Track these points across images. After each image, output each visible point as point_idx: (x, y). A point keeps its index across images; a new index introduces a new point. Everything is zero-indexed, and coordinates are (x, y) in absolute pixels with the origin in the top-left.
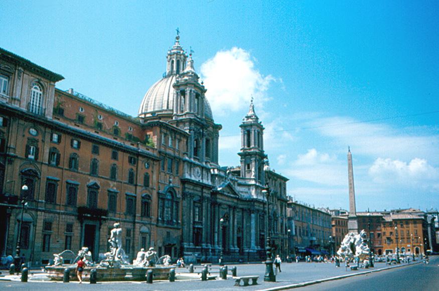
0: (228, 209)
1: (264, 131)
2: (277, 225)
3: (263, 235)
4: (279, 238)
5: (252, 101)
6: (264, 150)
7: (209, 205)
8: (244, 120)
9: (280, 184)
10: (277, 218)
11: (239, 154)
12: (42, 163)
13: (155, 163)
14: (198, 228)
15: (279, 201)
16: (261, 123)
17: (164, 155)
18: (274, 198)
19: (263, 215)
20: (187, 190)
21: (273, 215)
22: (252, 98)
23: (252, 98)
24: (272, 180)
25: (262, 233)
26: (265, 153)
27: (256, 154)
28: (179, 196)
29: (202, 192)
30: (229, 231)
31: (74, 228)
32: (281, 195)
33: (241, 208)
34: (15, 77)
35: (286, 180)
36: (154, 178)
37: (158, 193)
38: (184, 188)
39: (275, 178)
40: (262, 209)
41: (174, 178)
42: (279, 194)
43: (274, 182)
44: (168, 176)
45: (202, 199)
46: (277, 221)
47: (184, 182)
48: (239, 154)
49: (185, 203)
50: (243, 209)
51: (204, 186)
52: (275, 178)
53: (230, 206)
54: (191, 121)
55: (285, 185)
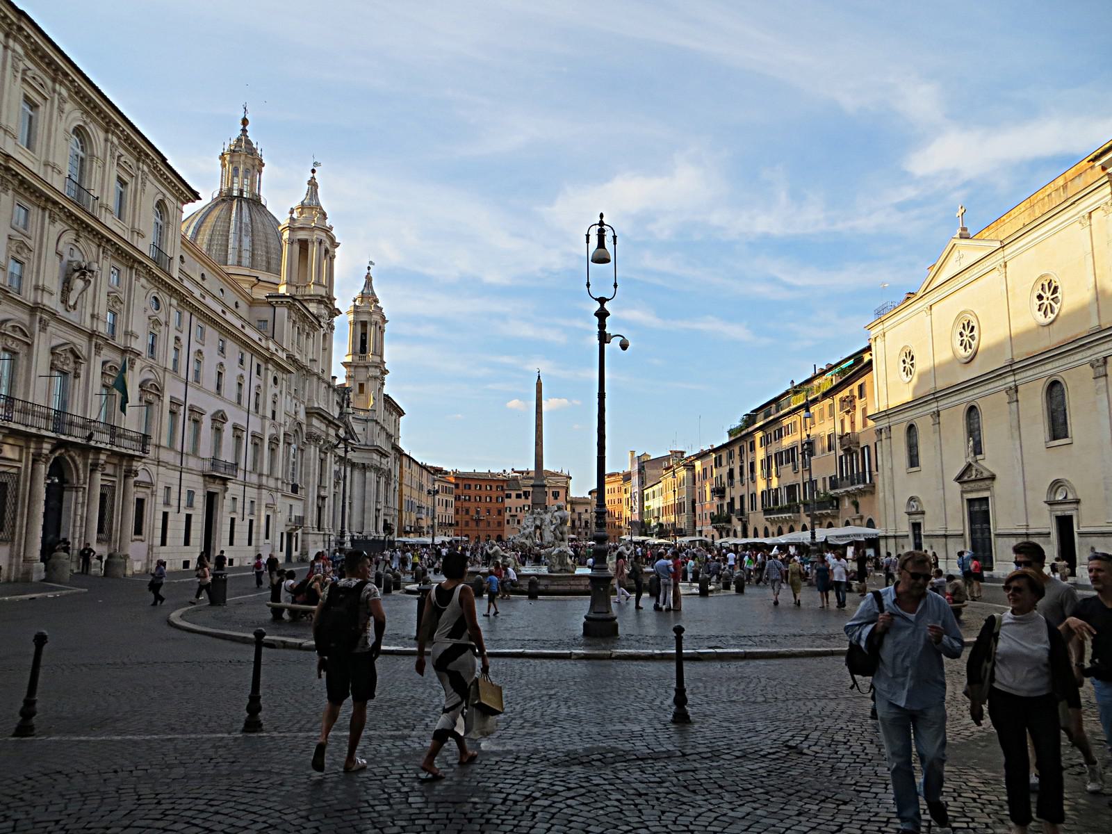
5: (369, 268)
8: (355, 301)
11: (345, 364)
12: (165, 369)
13: (284, 376)
20: (314, 430)
25: (379, 507)
26: (387, 366)
31: (196, 498)
34: (136, 184)
35: (401, 413)
36: (285, 404)
44: (294, 401)
48: (345, 364)
54: (320, 301)
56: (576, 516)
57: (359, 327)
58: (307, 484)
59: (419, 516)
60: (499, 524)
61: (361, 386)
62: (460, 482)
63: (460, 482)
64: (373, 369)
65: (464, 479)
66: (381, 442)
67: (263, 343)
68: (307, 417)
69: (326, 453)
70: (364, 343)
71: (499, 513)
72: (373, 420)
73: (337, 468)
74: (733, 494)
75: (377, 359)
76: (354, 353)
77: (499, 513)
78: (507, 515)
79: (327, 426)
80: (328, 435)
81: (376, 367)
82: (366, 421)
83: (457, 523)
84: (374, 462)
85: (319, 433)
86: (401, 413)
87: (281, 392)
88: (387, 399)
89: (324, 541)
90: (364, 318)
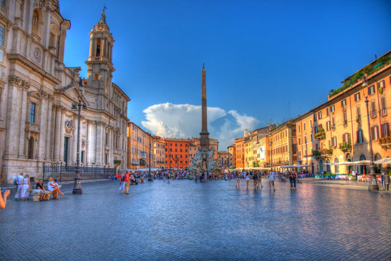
0: (73, 118)
3: (108, 150)
5: (104, 10)
6: (113, 62)
7: (51, 104)
8: (94, 26)
9: (123, 102)
14: (32, 132)
15: (122, 119)
18: (118, 115)
20: (17, 74)
21: (117, 131)
22: (105, 7)
23: (105, 7)
24: (117, 97)
25: (107, 148)
26: (113, 66)
30: (73, 141)
33: (87, 120)
38: (12, 70)
39: (120, 95)
42: (121, 112)
45: (41, 93)
46: (119, 137)
55: (127, 105)
56: (221, 159)
59: (143, 157)
60: (186, 162)
62: (167, 142)
63: (167, 142)
64: (104, 65)
65: (169, 141)
68: (11, 63)
69: (41, 101)
71: (186, 157)
72: (102, 95)
73: (70, 119)
74: (334, 134)
75: (106, 59)
76: (93, 55)
77: (186, 157)
78: (190, 158)
80: (42, 86)
81: (106, 64)
83: (166, 162)
84: (102, 120)
85: (27, 80)
86: (128, 99)
89: (38, 167)
90: (99, 36)
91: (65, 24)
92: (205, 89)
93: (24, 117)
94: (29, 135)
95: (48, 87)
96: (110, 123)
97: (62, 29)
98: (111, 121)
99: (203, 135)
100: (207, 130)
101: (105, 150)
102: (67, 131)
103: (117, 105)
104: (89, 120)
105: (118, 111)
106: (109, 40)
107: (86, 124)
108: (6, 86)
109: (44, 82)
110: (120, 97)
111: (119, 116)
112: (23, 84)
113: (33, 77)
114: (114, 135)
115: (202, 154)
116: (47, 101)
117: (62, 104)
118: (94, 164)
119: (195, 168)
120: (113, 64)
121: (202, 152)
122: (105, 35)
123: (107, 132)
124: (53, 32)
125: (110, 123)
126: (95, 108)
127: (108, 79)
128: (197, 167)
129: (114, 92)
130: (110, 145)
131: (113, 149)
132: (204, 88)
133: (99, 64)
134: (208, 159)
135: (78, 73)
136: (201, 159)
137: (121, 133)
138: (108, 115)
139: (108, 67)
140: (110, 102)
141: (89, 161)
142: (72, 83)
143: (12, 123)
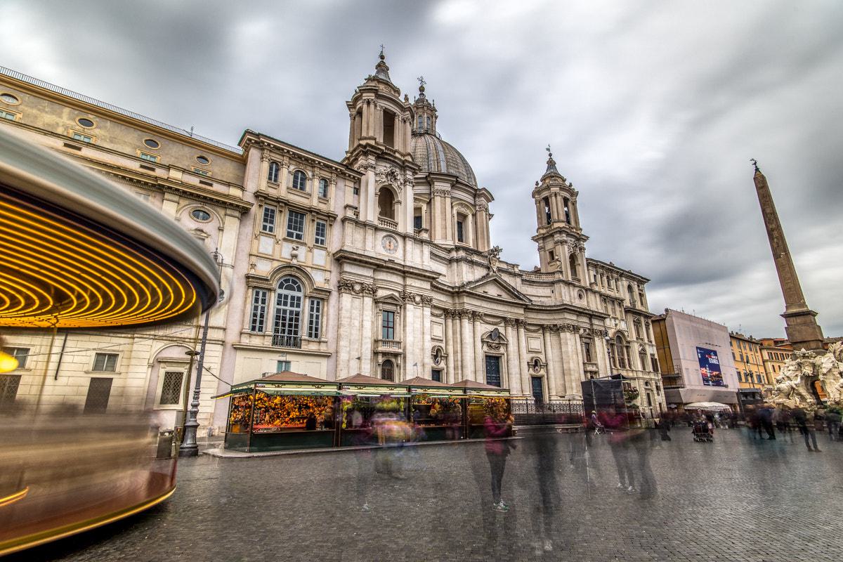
0: (503, 324)
1: (578, 199)
2: (628, 355)
4: (638, 378)
9: (630, 288)
10: (629, 342)
13: (229, 212)
14: (384, 354)
15: (630, 318)
16: (571, 185)
17: (275, 204)
19: (589, 334)
20: (346, 277)
25: (590, 368)
27: (561, 231)
28: (332, 286)
29: (405, 286)
32: (633, 302)
37: (248, 277)
40: (588, 326)
41: (311, 251)
42: (627, 303)
43: (613, 282)
46: (627, 347)
47: (341, 258)
49: (347, 298)
50: (542, 327)
51: (405, 273)
52: (615, 275)
53: (504, 319)
57: (543, 204)
58: (338, 338)
61: (552, 253)
64: (558, 235)
66: (594, 304)
67: (159, 172)
70: (549, 216)
73: (491, 328)
79: (404, 278)
82: (552, 283)
84: (569, 322)
85: (369, 282)
87: (221, 230)
88: (593, 264)
90: (545, 194)
91: (480, 196)
92: (774, 213)
93: (368, 334)
94: (381, 359)
95: (415, 285)
96: (592, 325)
97: (477, 203)
98: (595, 322)
99: (792, 319)
100: (804, 305)
101: (586, 372)
102: (490, 346)
103: (609, 293)
104: (543, 325)
105: (616, 303)
106: (568, 196)
107: (541, 331)
108: (335, 294)
109: (408, 279)
110: (617, 280)
111: (621, 311)
112: (362, 290)
113: (382, 276)
114: (610, 344)
115: (800, 365)
116: (421, 305)
117: (467, 307)
118: (564, 397)
119: (781, 400)
120: (581, 229)
121: (799, 360)
122: (554, 189)
123: (587, 341)
124: (463, 210)
125: (592, 325)
126: (553, 304)
127: (573, 258)
128: (788, 396)
129: (597, 273)
130: (600, 362)
131: (611, 369)
132: (768, 211)
133: (552, 235)
134: (821, 377)
135: (497, 257)
136: (797, 376)
137: (632, 336)
138: (581, 313)
139: (568, 235)
140: (586, 290)
141: (553, 393)
142: (488, 274)
143: (342, 343)
